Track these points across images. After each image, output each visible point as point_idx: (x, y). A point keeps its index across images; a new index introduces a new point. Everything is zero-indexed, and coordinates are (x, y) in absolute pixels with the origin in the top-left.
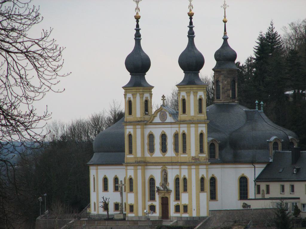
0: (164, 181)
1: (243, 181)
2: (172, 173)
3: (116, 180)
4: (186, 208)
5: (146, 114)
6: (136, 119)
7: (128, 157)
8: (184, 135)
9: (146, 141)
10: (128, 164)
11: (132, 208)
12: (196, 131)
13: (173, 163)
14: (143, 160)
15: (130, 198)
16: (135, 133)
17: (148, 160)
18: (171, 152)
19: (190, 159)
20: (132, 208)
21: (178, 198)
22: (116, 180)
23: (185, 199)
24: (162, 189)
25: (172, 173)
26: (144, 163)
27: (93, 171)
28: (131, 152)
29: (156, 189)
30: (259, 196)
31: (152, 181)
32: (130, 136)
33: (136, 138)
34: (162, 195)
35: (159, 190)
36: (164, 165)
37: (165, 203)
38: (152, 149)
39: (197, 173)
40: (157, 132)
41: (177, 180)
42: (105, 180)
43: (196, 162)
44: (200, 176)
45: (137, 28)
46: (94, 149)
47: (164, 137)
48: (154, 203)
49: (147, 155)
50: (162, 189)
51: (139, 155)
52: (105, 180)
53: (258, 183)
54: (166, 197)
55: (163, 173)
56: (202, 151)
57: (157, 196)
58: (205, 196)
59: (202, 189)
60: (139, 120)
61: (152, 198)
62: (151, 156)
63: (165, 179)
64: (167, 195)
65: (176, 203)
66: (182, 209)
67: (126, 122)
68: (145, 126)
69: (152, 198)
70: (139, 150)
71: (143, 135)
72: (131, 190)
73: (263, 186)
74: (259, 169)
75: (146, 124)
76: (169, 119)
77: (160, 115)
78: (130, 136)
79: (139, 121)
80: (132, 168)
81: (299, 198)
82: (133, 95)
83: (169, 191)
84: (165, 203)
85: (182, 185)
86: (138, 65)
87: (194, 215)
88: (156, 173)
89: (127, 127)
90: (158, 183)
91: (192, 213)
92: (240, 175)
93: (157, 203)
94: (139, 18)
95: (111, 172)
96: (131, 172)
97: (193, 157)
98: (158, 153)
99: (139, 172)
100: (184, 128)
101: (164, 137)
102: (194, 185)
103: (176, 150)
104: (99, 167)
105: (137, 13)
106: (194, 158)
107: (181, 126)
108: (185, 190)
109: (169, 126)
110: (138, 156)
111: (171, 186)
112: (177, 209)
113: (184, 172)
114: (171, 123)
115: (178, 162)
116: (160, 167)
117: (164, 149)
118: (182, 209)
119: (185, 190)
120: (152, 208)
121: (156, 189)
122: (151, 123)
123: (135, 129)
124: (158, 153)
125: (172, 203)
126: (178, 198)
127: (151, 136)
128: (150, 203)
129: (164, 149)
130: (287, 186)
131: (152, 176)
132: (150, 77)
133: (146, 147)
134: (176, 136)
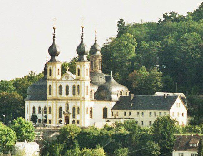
1: (105, 110)
4: (78, 122)
7: (49, 96)
8: (78, 86)
9: (58, 89)
10: (49, 100)
13: (72, 100)
16: (53, 85)
17: (59, 98)
21: (74, 117)
23: (78, 117)
24: (66, 112)
26: (57, 99)
27: (27, 103)
28: (50, 94)
29: (63, 113)
30: (113, 117)
31: (61, 109)
32: (50, 86)
34: (66, 116)
35: (64, 113)
38: (61, 93)
41: (74, 109)
47: (67, 87)
48: (61, 119)
49: (59, 96)
50: (66, 112)
51: (54, 96)
52: (34, 108)
53: (113, 111)
54: (68, 117)
57: (63, 116)
61: (61, 117)
66: (76, 122)
67: (48, 79)
69: (61, 117)
70: (55, 93)
71: (56, 85)
73: (115, 112)
74: (114, 104)
78: (50, 86)
81: (133, 118)
82: (52, 66)
86: (53, 52)
88: (63, 105)
90: (64, 110)
92: (104, 107)
93: (63, 119)
99: (54, 104)
101: (67, 87)
103: (74, 94)
107: (77, 81)
111: (71, 111)
112: (74, 122)
114: (71, 80)
115: (75, 99)
116: (66, 102)
117: (67, 93)
118: (76, 122)
119: (78, 113)
121: (63, 113)
126: (74, 117)
127: (61, 87)
129: (67, 93)
130: (128, 112)
132: (57, 58)
133: (58, 92)
134: (74, 87)
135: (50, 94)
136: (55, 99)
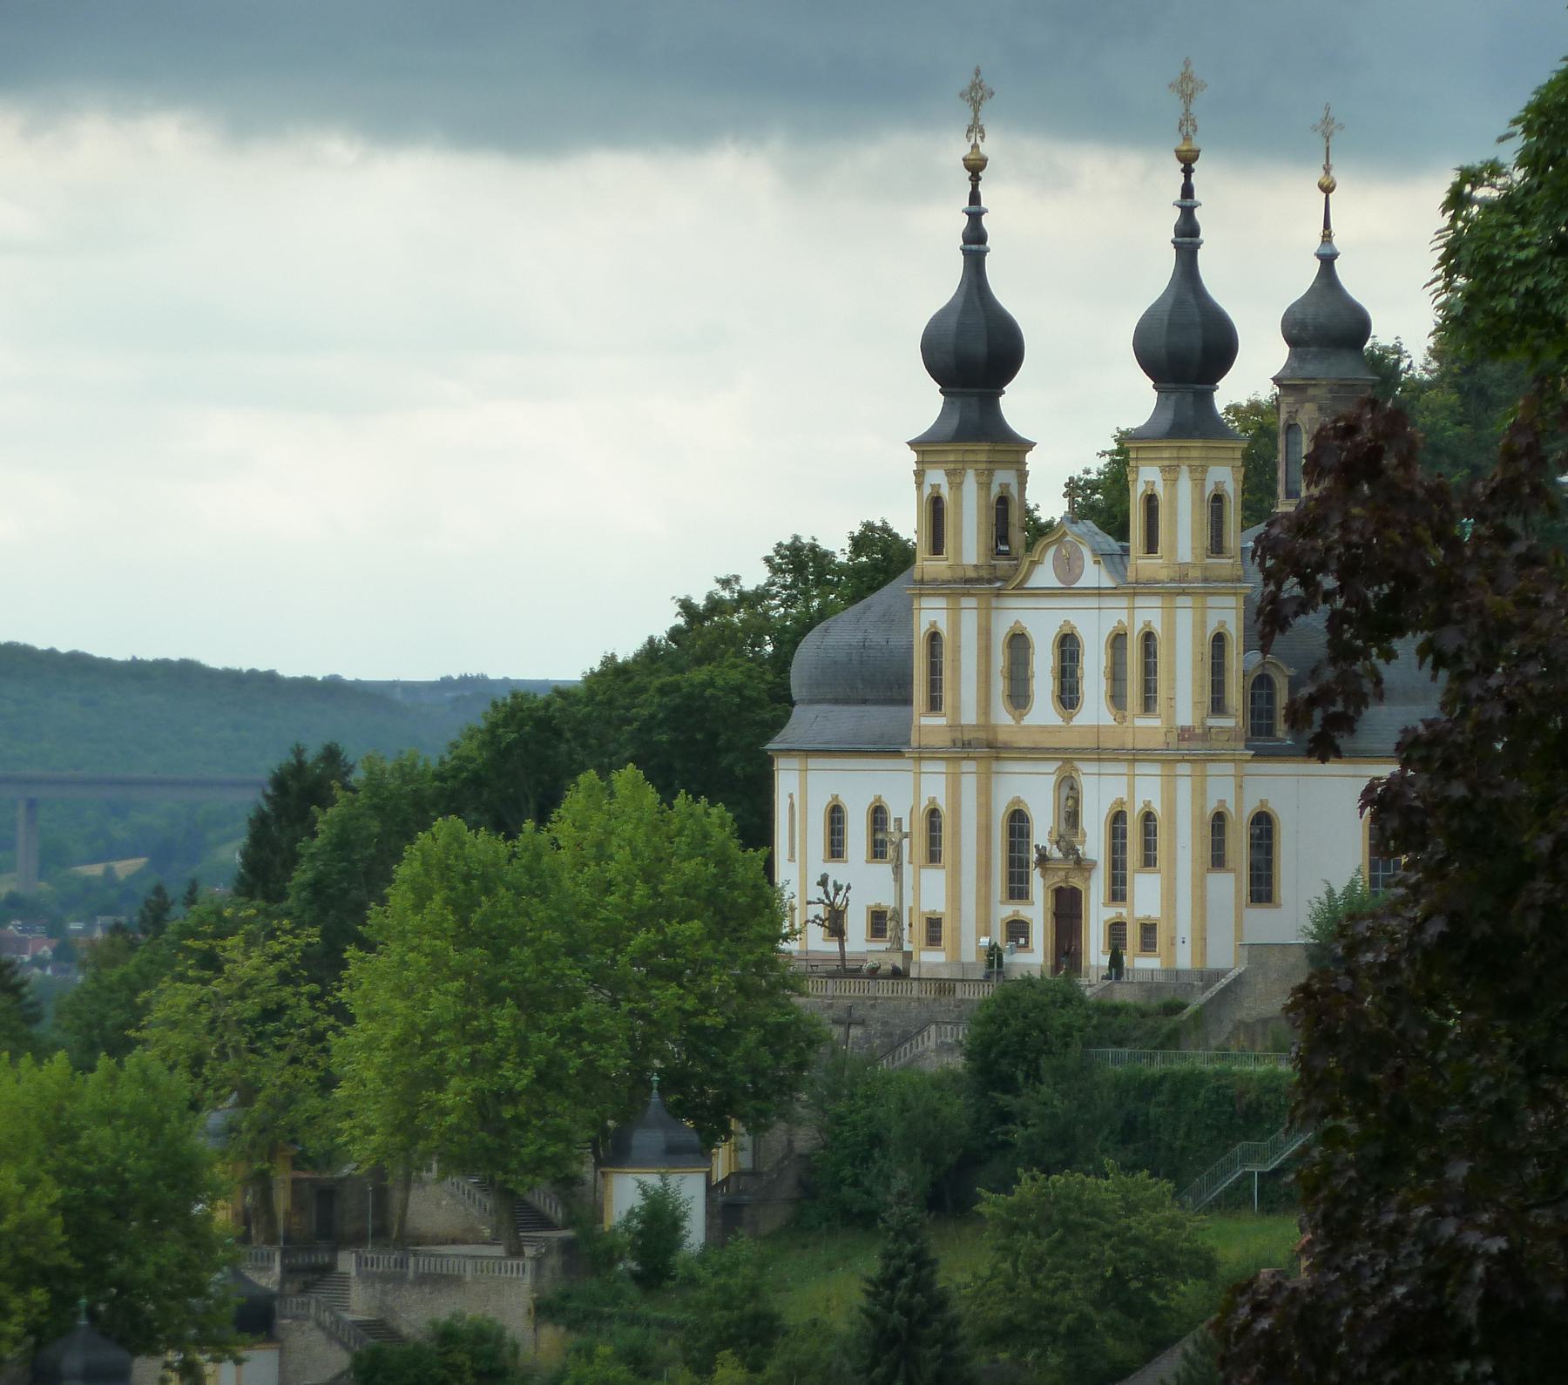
0: (1067, 820)
2: (1101, 792)
3: (878, 815)
5: (1000, 553)
6: (959, 574)
9: (1000, 660)
10: (924, 754)
11: (934, 924)
12: (1201, 624)
13: (1100, 753)
14: (982, 735)
15: (930, 891)
16: (955, 627)
17: (1002, 737)
18: (1094, 708)
19: (1173, 738)
20: (934, 924)
21: (1118, 892)
22: (878, 815)
24: (1057, 854)
25: (1101, 792)
26: (984, 749)
27: (787, 781)
28: (935, 704)
29: (1034, 856)
31: (1018, 822)
32: (934, 637)
33: (957, 649)
34: (1057, 880)
35: (1043, 859)
36: (1067, 759)
37: (1067, 908)
38: (1019, 696)
39: (1200, 793)
40: (1043, 625)
41: (1118, 819)
42: (836, 816)
43: (1189, 748)
44: (1211, 807)
45: (974, 208)
46: (796, 693)
47: (1068, 646)
49: (1003, 716)
51: (970, 716)
52: (836, 816)
55: (1065, 791)
56: (1218, 706)
57: (1038, 885)
58: (1228, 886)
59: (1218, 860)
60: (971, 574)
61: (1018, 890)
62: (1019, 719)
63: (1071, 818)
64: (1076, 882)
65: (1111, 913)
68: (994, 602)
70: (968, 695)
71: (985, 633)
72: (934, 857)
75: (998, 594)
76: (1093, 574)
77: (1055, 558)
78: (934, 637)
79: (967, 581)
80: (941, 767)
82: (949, 473)
83: (1082, 865)
84: (1067, 908)
85: (1134, 838)
86: (975, 355)
87: (1184, 959)
89: (926, 602)
90: (1042, 832)
91: (1171, 955)
93: (1037, 911)
94: (982, 167)
95: (858, 786)
96: (934, 784)
97: (1183, 729)
98: (1043, 709)
99: (969, 784)
100: (1148, 614)
101: (1068, 646)
102: (1184, 842)
103: (1117, 698)
104: (813, 763)
105: (975, 147)
106: (1185, 734)
107: (1140, 602)
108: (1149, 861)
109: (1093, 602)
110: (963, 722)
111: (1094, 845)
112: (1116, 931)
113: (1148, 789)
114: (1099, 592)
116: (1052, 767)
117: (1068, 696)
118: (1133, 936)
119: (1149, 861)
120: (1018, 930)
122: (1022, 590)
123: (955, 611)
124: (1043, 709)
125: (1097, 914)
126: (1118, 892)
127: (1019, 643)
128: (1006, 911)
129: (1068, 696)
131: (1018, 801)
132: (1018, 404)
133: (1000, 685)
134: (1118, 641)
135: (935, 704)
136: (966, 744)
